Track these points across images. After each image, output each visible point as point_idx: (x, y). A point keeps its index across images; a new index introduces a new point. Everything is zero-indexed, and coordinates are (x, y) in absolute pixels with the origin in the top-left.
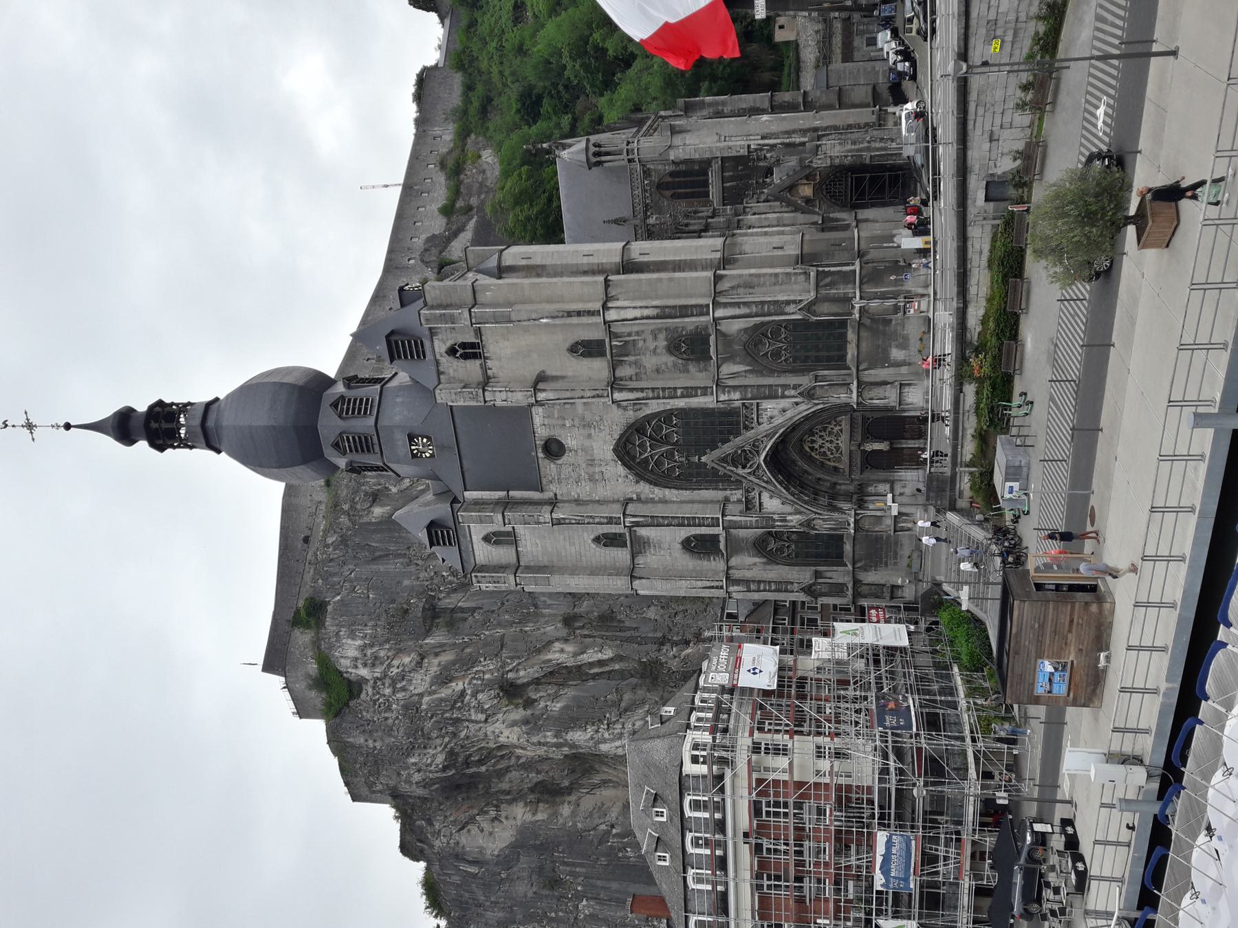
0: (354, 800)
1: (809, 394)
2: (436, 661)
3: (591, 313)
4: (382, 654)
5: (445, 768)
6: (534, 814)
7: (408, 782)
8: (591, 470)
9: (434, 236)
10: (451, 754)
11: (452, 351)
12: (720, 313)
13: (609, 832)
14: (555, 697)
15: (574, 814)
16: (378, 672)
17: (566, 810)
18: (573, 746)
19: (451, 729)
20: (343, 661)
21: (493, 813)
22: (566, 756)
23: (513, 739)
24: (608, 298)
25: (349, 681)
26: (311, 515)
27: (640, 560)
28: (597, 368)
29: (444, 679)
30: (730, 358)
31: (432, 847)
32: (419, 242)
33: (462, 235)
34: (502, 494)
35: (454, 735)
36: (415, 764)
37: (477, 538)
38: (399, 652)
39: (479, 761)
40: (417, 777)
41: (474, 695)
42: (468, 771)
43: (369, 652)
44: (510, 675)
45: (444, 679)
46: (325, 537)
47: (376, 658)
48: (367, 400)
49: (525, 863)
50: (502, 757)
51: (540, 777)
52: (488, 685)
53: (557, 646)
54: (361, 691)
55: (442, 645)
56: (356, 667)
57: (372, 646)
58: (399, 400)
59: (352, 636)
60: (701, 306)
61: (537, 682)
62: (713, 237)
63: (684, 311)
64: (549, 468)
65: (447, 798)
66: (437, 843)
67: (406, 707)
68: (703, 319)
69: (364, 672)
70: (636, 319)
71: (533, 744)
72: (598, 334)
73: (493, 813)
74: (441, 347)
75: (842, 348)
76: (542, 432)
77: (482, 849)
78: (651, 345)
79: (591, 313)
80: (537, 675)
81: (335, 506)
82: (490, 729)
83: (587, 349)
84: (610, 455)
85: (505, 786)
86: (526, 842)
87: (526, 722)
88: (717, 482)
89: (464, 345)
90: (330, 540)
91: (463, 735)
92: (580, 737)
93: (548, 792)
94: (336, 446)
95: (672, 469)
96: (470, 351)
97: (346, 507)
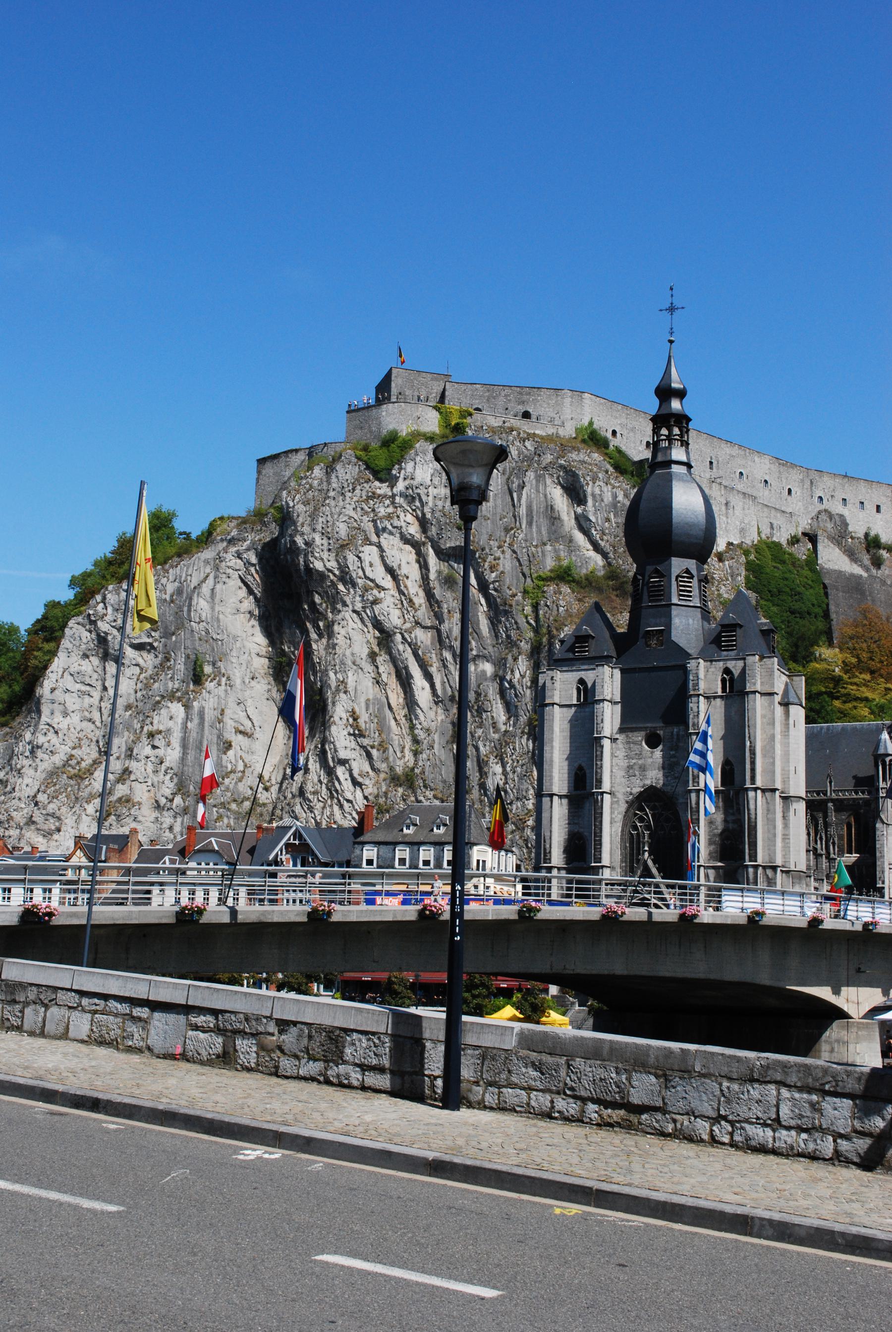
0: (262, 462)
5: (309, 570)
8: (636, 767)
9: (847, 525)
10: (322, 576)
20: (411, 464)
24: (764, 791)
26: (552, 421)
27: (565, 801)
31: (225, 550)
33: (846, 559)
34: (618, 698)
37: (582, 674)
44: (398, 637)
46: (531, 436)
47: (414, 498)
48: (690, 596)
54: (381, 481)
56: (405, 479)
58: (691, 621)
60: (756, 856)
62: (808, 860)
64: (639, 737)
66: (229, 556)
68: (747, 857)
69: (401, 486)
70: (749, 810)
74: (730, 664)
81: (564, 446)
84: (648, 782)
88: (626, 862)
90: (527, 444)
91: (341, 587)
95: (635, 828)
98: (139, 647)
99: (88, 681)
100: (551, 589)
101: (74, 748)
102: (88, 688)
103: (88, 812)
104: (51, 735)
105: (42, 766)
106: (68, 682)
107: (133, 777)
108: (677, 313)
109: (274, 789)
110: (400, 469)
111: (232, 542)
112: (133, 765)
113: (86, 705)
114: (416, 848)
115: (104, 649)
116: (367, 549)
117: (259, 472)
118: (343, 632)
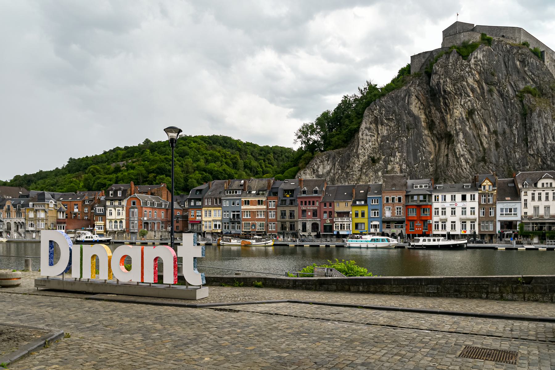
2: (477, 86)
4: (479, 67)
5: (445, 91)
7: (440, 78)
10: (450, 93)
13: (423, 146)
14: (470, 128)
15: (426, 135)
16: (472, 66)
17: (426, 132)
21: (421, 107)
29: (473, 90)
31: (411, 86)
35: (456, 94)
36: (447, 80)
38: (479, 73)
39: (446, 103)
40: (442, 81)
41: (469, 100)
45: (473, 90)
49: (411, 119)
51: (437, 123)
52: (472, 106)
54: (465, 60)
55: (483, 88)
56: (474, 58)
57: (482, 63)
59: (484, 56)
65: (427, 91)
67: (462, 76)
69: (473, 61)
71: (455, 121)
77: (412, 104)
80: (476, 122)
85: (433, 111)
86: (416, 119)
87: (463, 118)
90: (508, 46)
93: (431, 126)
98: (388, 119)
104: (363, 150)
105: (361, 160)
110: (472, 55)
115: (376, 121)
118: (458, 112)
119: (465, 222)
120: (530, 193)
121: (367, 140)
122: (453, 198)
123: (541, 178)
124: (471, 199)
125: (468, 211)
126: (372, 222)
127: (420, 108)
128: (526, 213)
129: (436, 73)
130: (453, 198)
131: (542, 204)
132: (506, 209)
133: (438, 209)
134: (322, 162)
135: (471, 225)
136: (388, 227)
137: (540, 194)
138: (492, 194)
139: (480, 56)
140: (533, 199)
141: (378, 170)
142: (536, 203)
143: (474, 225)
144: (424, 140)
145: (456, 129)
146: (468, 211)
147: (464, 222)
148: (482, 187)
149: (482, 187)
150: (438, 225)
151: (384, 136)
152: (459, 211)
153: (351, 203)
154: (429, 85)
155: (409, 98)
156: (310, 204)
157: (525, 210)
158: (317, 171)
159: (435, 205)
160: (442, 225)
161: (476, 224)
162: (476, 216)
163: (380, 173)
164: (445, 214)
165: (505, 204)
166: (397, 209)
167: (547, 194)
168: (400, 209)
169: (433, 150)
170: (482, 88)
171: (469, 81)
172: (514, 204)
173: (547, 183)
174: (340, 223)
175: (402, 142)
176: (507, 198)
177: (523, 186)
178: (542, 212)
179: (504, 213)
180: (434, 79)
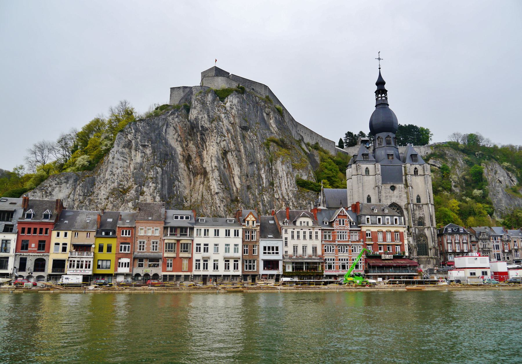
0: (171, 88)
1: (415, 248)
3: (430, 201)
4: (233, 111)
5: (202, 127)
6: (180, 155)
7: (199, 113)
11: (416, 168)
12: (432, 229)
13: (178, 180)
15: (182, 168)
16: (228, 109)
17: (182, 165)
18: (213, 171)
19: (215, 131)
22: (205, 168)
23: (211, 152)
25: (225, 98)
28: (415, 201)
29: (228, 131)
30: (419, 231)
31: (169, 116)
32: (302, 134)
38: (234, 117)
39: (203, 138)
40: (200, 117)
42: (198, 134)
43: (234, 107)
45: (228, 131)
47: (232, 109)
50: (203, 146)
51: (193, 158)
53: (239, 169)
59: (238, 102)
61: (228, 161)
63: (432, 221)
64: (388, 186)
66: (170, 118)
69: (228, 104)
72: (423, 201)
73: (179, 139)
74: (417, 166)
75: (421, 255)
76: (397, 186)
78: (421, 213)
79: (430, 201)
82: (215, 144)
83: (419, 200)
84: (393, 201)
85: (191, 145)
89: (417, 171)
92: (216, 173)
93: (188, 160)
94: (388, 136)
96: (416, 172)
97: (266, 105)
98: (144, 146)
99: (125, 156)
100: (271, 143)
101: (122, 181)
102: (125, 159)
103: (129, 206)
104: (112, 176)
106: (117, 156)
107: (145, 194)
108: (381, 60)
109: (189, 202)
111: (171, 114)
112: (145, 189)
113: (125, 166)
114: (383, 217)
116: (221, 123)
117: (171, 92)
119: (228, 261)
120: (290, 231)
121: (119, 166)
122: (217, 233)
123: (299, 217)
124: (235, 235)
125: (232, 248)
126: (120, 258)
127: (177, 140)
128: (286, 252)
129: (195, 108)
130: (217, 233)
131: (300, 243)
132: (269, 248)
133: (200, 245)
134: (58, 184)
135: (235, 264)
136: (141, 266)
137: (298, 232)
138: (255, 230)
139: (235, 101)
140: (293, 237)
141: (128, 201)
142: (295, 242)
143: (237, 264)
144: (180, 174)
145: (212, 167)
146: (232, 248)
147: (227, 260)
148: (246, 222)
149: (246, 222)
150: (199, 264)
151: (137, 163)
152: (222, 248)
153: (93, 234)
154: (188, 119)
155: (167, 127)
156: (35, 232)
157: (286, 249)
158: (51, 194)
159: (197, 240)
160: (204, 264)
161: (240, 263)
162: (239, 254)
163: (130, 204)
164: (207, 251)
165: (268, 242)
166: (153, 243)
167: (305, 232)
168: (157, 243)
169: (189, 185)
170: (235, 131)
171: (224, 122)
172: (276, 242)
173: (304, 222)
174: (76, 260)
175: (157, 173)
176: (269, 236)
177: (284, 223)
178: (300, 252)
179: (267, 251)
180: (193, 114)
